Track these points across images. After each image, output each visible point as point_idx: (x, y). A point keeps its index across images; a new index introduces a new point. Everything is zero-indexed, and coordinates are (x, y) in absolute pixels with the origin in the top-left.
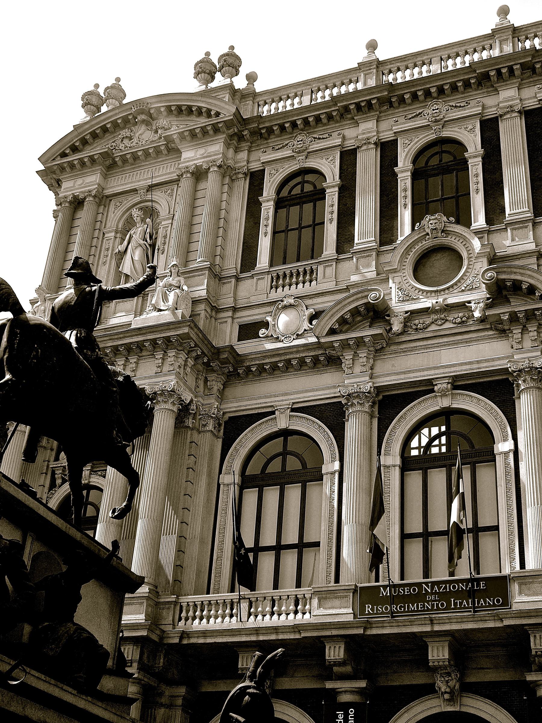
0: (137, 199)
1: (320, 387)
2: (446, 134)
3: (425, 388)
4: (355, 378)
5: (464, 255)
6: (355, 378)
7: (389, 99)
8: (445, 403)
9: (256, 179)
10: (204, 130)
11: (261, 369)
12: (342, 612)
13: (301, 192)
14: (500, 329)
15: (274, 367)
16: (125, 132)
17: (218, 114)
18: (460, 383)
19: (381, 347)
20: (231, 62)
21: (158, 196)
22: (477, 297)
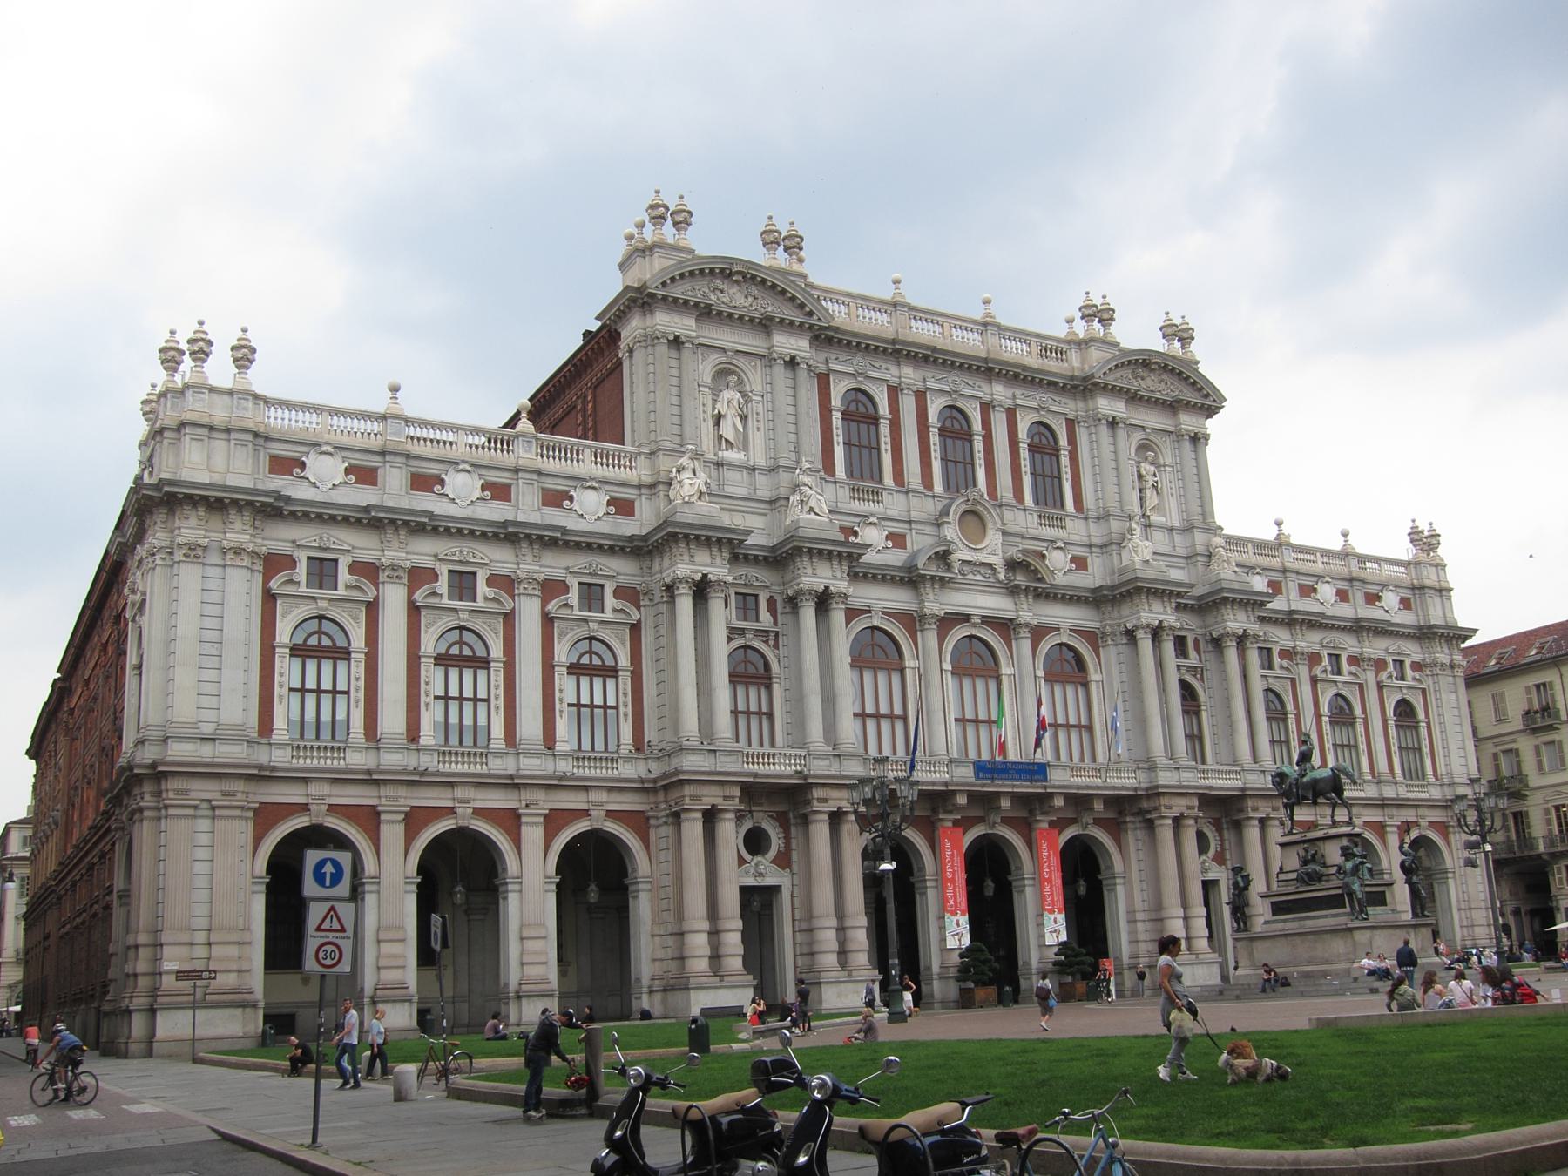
0: (724, 359)
1: (899, 599)
2: (958, 404)
3: (966, 618)
4: (936, 603)
5: (990, 525)
6: (936, 603)
7: (928, 357)
8: (974, 632)
9: (823, 381)
10: (802, 324)
11: (865, 575)
12: (965, 774)
13: (861, 413)
14: (1013, 591)
15: (874, 576)
16: (718, 283)
17: (811, 314)
18: (988, 621)
19: (943, 582)
20: (793, 245)
21: (741, 362)
22: (997, 560)
